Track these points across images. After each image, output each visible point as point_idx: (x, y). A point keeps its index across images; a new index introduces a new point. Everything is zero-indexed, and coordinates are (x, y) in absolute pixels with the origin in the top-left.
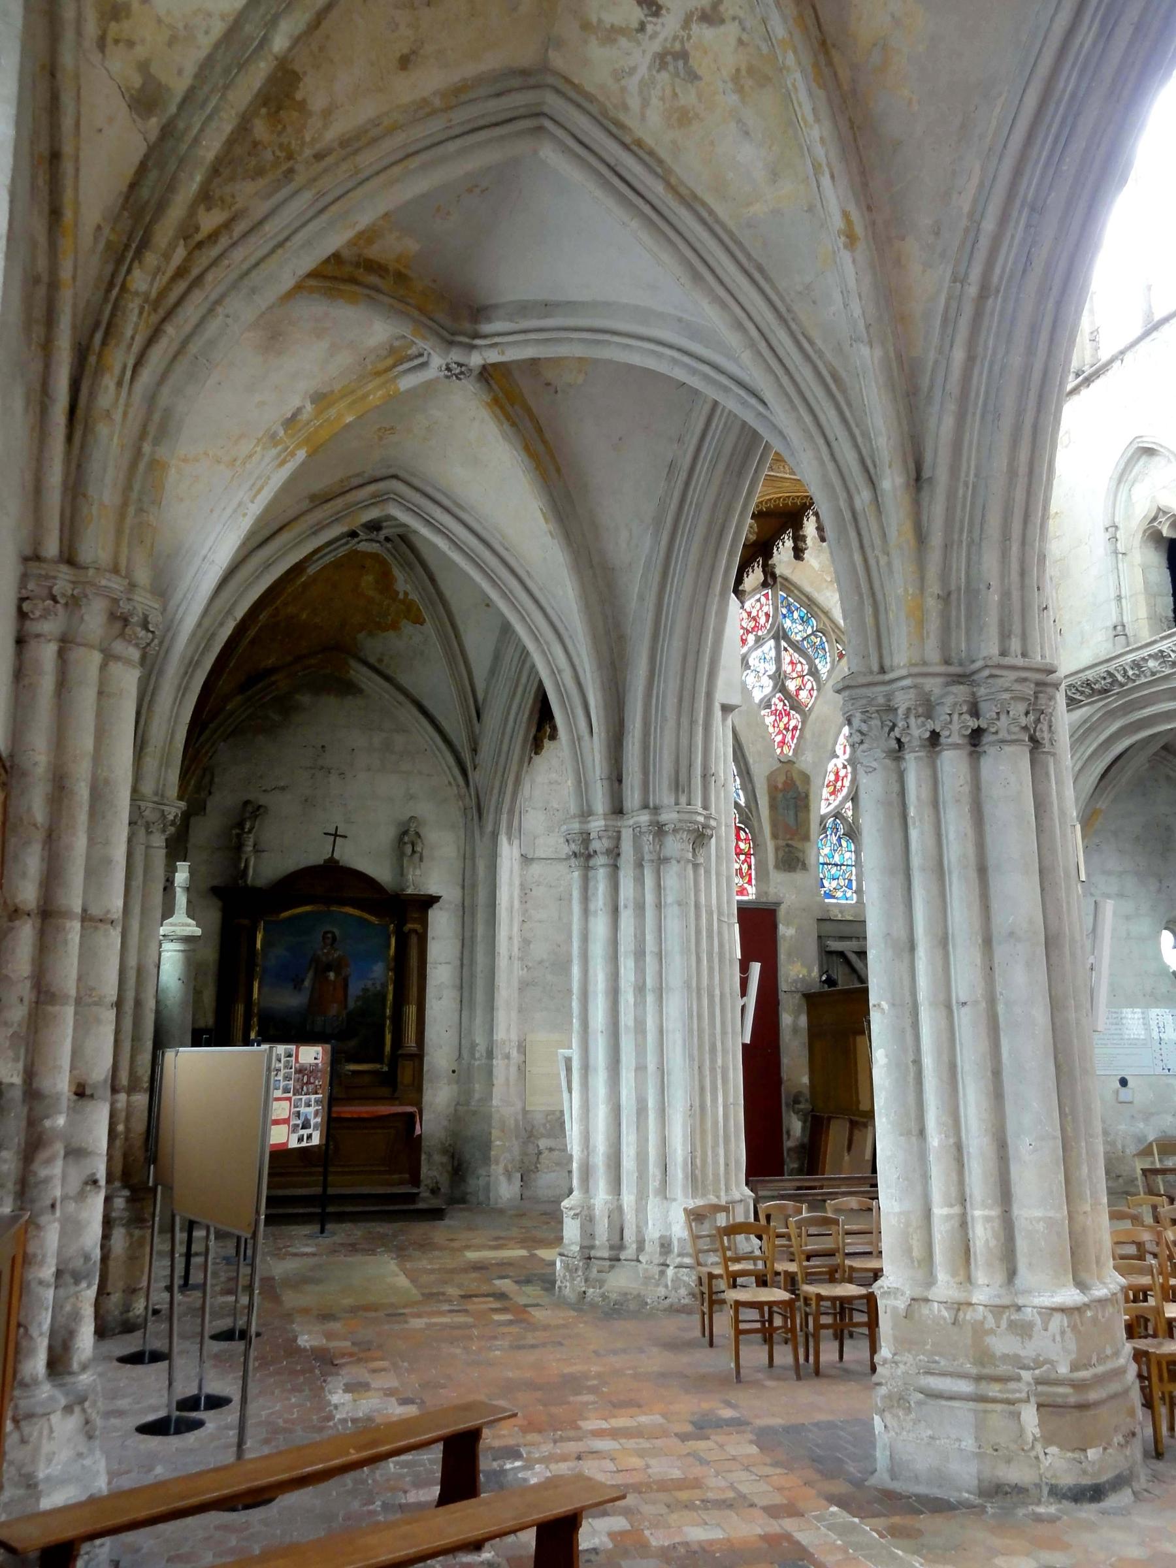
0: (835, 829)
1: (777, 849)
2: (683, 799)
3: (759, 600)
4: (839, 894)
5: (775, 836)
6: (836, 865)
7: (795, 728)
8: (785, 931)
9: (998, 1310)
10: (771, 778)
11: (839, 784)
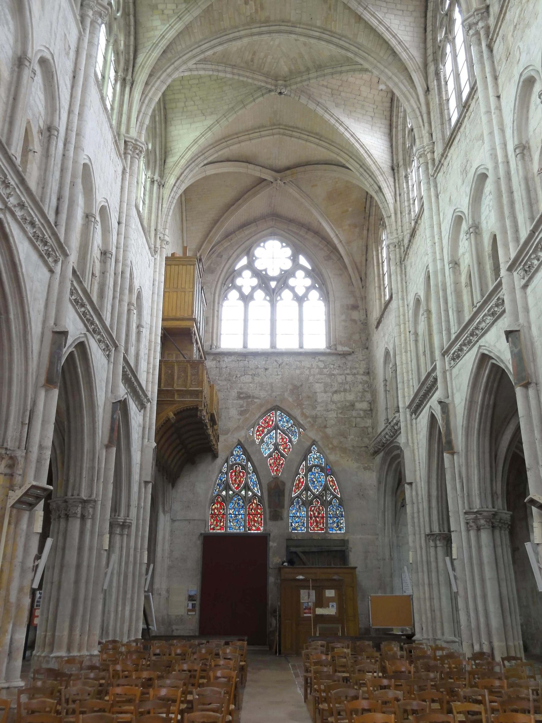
0: (298, 503)
1: (270, 512)
2: (117, 514)
3: (269, 415)
4: (299, 529)
5: (269, 507)
6: (298, 517)
7: (282, 464)
8: (272, 544)
9: (45, 657)
10: (269, 485)
11: (300, 484)
